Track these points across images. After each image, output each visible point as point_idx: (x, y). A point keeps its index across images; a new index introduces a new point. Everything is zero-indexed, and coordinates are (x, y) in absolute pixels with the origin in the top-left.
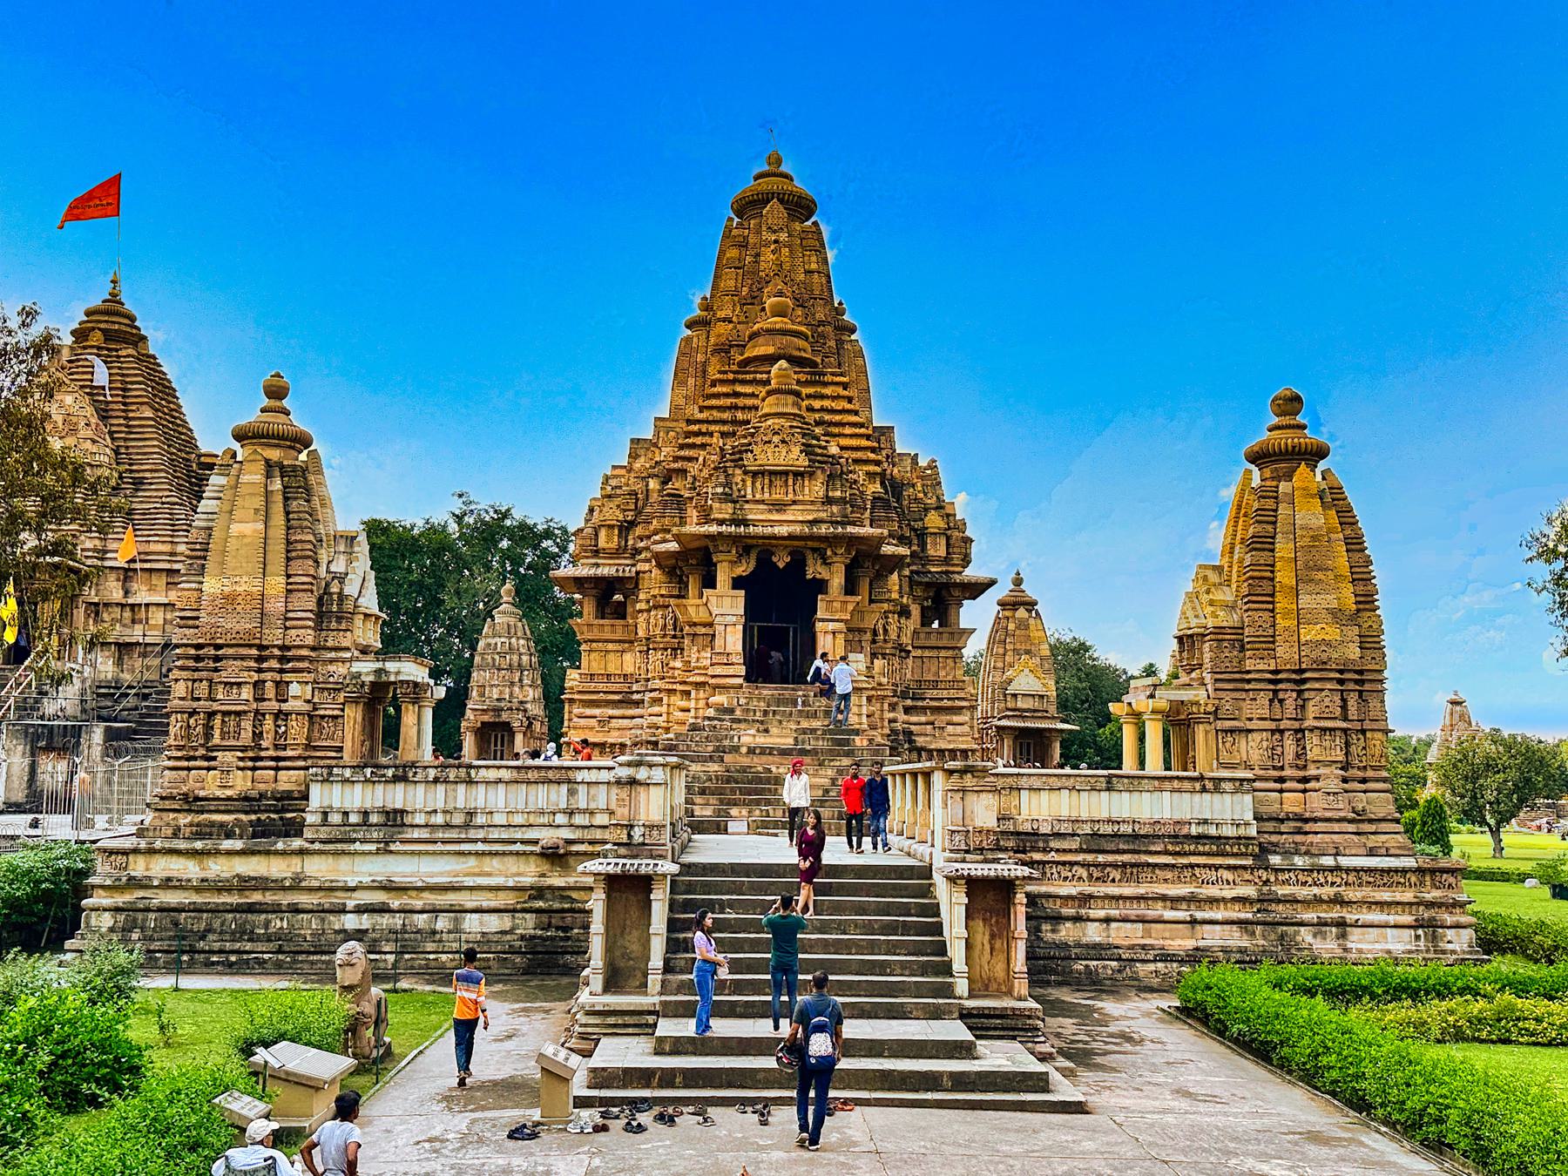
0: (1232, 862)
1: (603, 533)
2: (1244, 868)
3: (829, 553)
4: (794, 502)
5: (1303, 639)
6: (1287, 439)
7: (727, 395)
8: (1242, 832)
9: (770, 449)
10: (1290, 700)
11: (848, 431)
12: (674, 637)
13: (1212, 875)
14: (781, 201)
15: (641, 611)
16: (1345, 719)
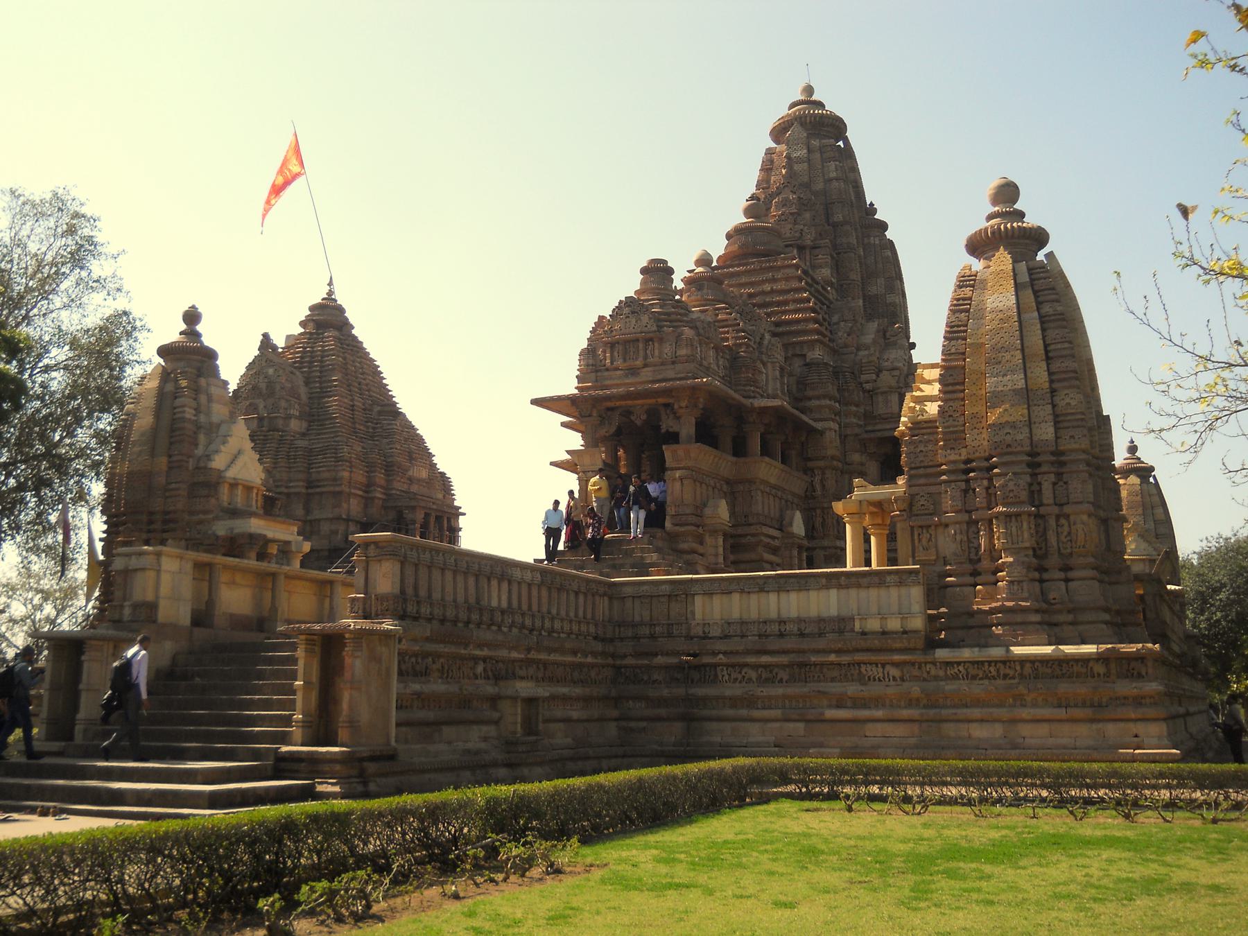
0: (897, 658)
4: (646, 366)
11: (791, 307)
13: (877, 672)
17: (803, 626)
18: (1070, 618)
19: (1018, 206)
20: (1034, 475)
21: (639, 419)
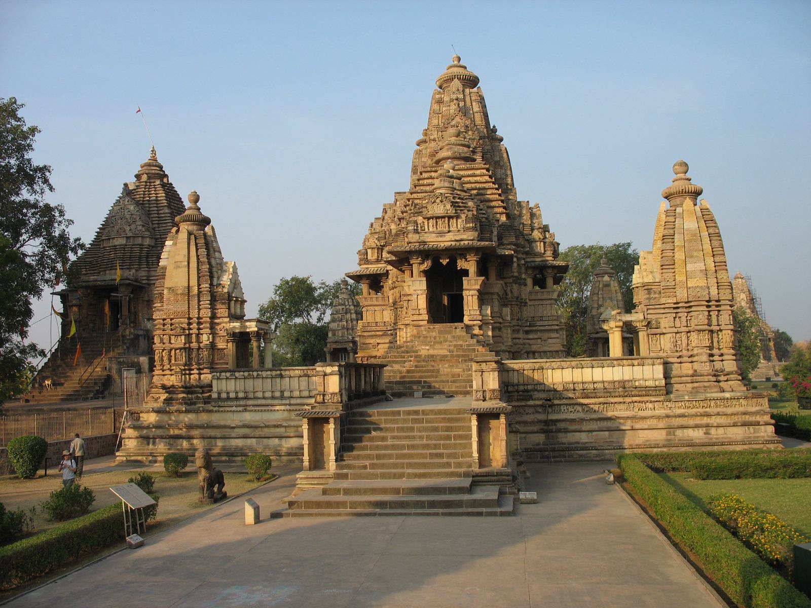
0: (653, 399)
1: (369, 251)
2: (659, 401)
4: (449, 232)
5: (689, 286)
6: (681, 185)
8: (657, 383)
9: (435, 205)
10: (683, 315)
14: (459, 79)
16: (710, 326)
17: (606, 385)
18: (725, 378)
19: (688, 175)
20: (709, 311)
21: (445, 262)
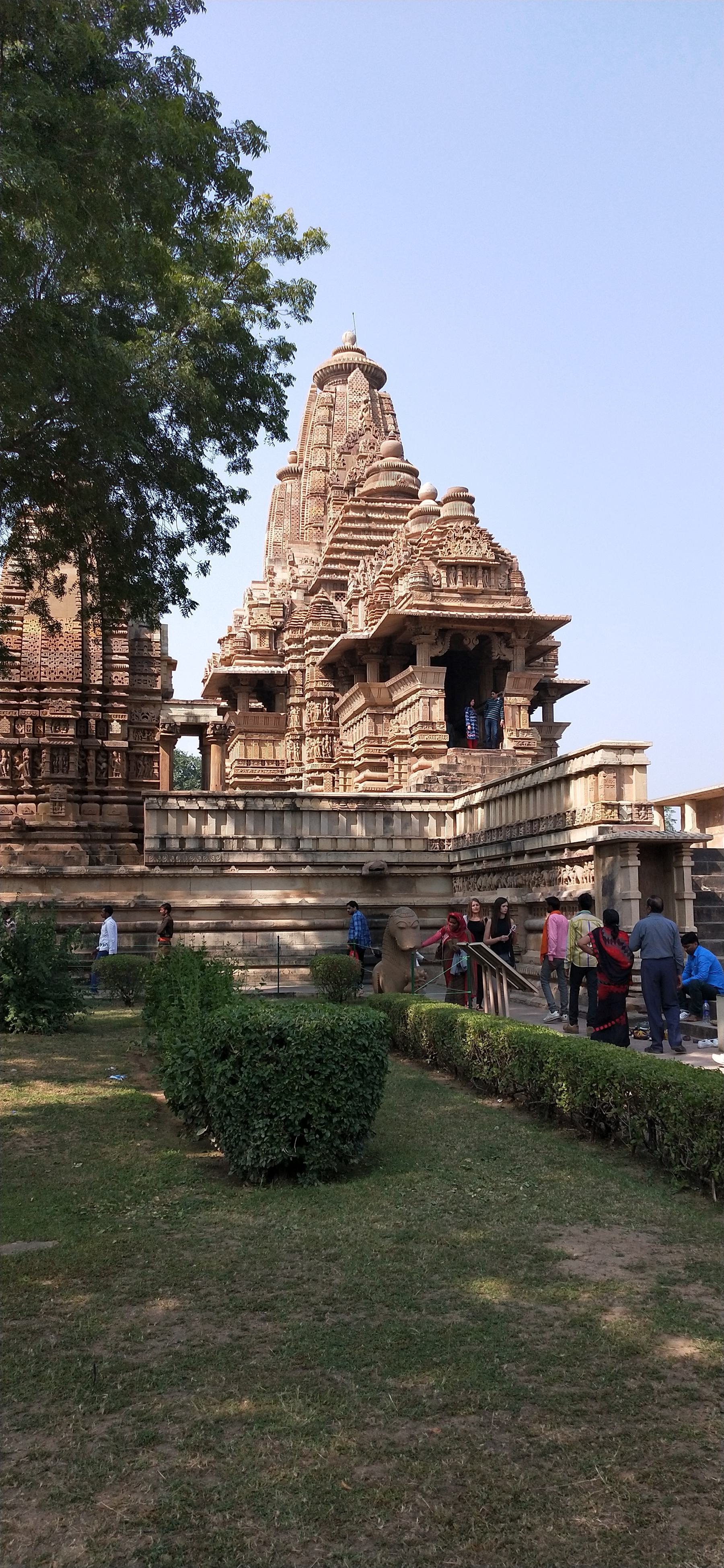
3: (513, 636)
7: (360, 520)
12: (330, 724)
14: (362, 370)
15: (294, 705)
21: (471, 644)
